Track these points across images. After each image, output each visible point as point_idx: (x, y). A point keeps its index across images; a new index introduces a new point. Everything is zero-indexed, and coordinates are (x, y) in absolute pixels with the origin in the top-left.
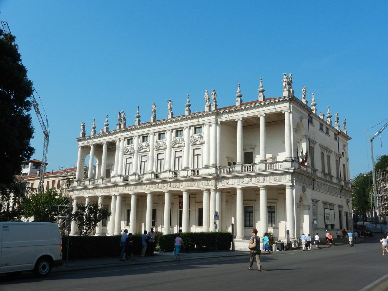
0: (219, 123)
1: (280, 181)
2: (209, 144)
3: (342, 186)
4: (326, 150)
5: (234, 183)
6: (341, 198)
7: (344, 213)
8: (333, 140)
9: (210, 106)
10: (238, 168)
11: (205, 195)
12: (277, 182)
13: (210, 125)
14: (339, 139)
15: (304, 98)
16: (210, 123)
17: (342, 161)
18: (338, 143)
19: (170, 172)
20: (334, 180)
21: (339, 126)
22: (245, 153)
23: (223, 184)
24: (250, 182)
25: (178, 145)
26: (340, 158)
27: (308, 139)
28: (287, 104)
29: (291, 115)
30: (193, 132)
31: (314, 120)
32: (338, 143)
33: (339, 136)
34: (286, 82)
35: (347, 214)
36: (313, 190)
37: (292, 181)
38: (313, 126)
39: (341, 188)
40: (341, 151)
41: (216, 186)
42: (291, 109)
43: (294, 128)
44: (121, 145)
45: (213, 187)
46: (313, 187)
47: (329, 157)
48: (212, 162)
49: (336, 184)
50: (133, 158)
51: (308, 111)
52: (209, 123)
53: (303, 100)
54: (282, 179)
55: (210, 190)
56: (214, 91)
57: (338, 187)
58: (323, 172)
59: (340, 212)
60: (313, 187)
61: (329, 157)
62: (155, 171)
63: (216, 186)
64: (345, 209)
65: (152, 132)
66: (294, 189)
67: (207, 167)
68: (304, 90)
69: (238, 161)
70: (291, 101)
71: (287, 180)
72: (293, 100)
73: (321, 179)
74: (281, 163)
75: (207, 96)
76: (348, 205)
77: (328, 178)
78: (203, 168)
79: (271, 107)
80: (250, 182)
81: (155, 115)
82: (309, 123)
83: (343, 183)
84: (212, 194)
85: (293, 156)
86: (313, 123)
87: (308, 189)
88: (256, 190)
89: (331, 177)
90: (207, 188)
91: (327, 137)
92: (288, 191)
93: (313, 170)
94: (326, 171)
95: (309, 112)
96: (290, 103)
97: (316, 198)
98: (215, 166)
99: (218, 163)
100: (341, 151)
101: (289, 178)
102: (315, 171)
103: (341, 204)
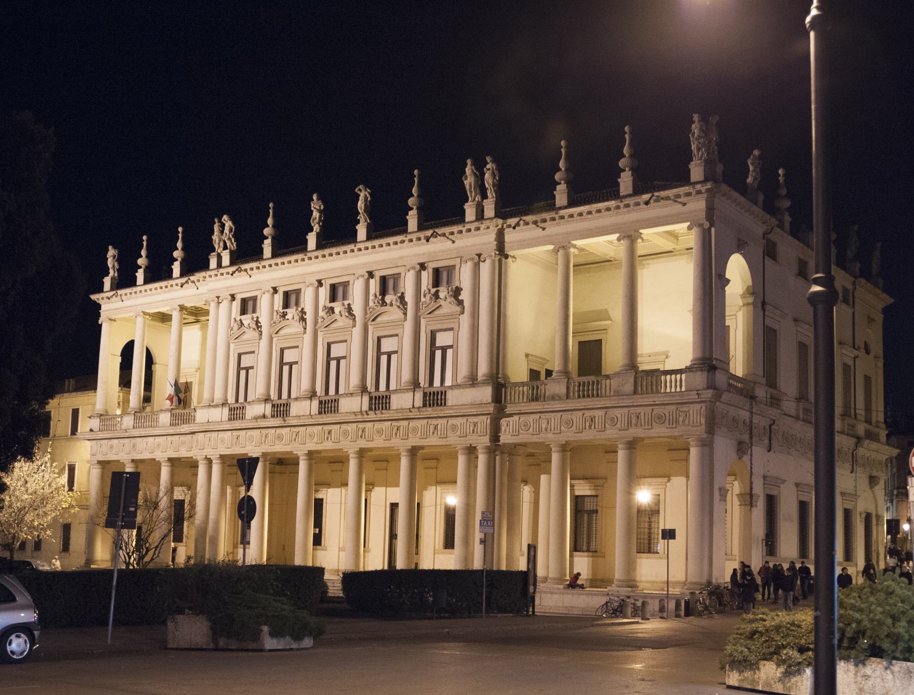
5: (546, 429)
16: (479, 255)
22: (580, 343)
30: (431, 282)
36: (769, 451)
50: (256, 352)
52: (477, 255)
62: (231, 399)
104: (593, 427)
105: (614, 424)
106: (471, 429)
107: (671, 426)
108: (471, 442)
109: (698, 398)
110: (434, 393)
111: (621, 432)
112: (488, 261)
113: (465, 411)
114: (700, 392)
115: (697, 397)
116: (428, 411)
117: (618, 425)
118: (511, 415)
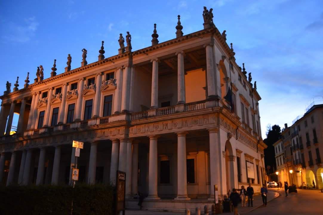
1: (202, 124)
2: (121, 88)
5: (147, 130)
10: (151, 113)
11: (114, 145)
14: (253, 97)
16: (123, 66)
19: (78, 123)
20: (252, 134)
24: (165, 128)
26: (255, 114)
36: (237, 139)
38: (234, 73)
40: (255, 109)
41: (127, 134)
45: (123, 136)
48: (123, 108)
54: (205, 122)
55: (119, 140)
57: (255, 141)
61: (247, 110)
63: (127, 134)
67: (118, 114)
69: (152, 104)
70: (213, 34)
74: (203, 104)
77: (248, 130)
78: (113, 115)
80: (165, 128)
84: (122, 144)
87: (232, 137)
88: (174, 137)
90: (116, 137)
94: (246, 122)
95: (230, 56)
97: (240, 149)
98: (126, 112)
103: (257, 158)
104: (167, 128)
105: (175, 126)
106: (117, 132)
107: (201, 125)
108: (117, 137)
109: (213, 111)
110: (104, 119)
111: (179, 129)
112: (126, 68)
113: (115, 124)
114: (213, 108)
115: (211, 111)
116: (100, 126)
117: (178, 127)
118: (133, 126)
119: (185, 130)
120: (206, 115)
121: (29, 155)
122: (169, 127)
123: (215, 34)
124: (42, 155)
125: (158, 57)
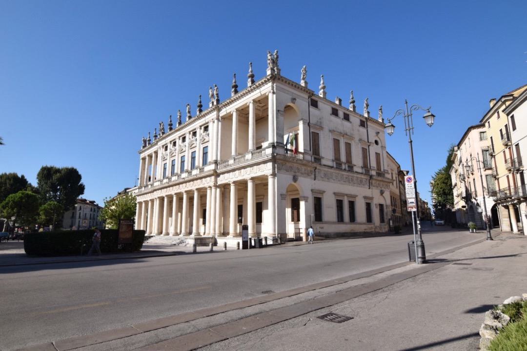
0: (220, 118)
2: (212, 140)
3: (371, 177)
4: (343, 136)
6: (369, 188)
7: (374, 206)
8: (358, 127)
9: (213, 103)
11: (208, 191)
12: (261, 173)
13: (214, 122)
14: (368, 126)
15: (303, 79)
17: (373, 149)
18: (367, 131)
21: (368, 113)
23: (222, 180)
25: (193, 146)
26: (369, 146)
27: (307, 124)
28: (270, 84)
29: (275, 96)
31: (320, 104)
32: (367, 131)
33: (368, 123)
34: (269, 60)
35: (381, 206)
37: (274, 168)
39: (369, 178)
41: (216, 181)
42: (275, 88)
43: (278, 111)
44: (161, 152)
46: (315, 177)
47: (348, 146)
49: (362, 173)
51: (307, 92)
53: (302, 83)
56: (216, 86)
58: (337, 159)
59: (368, 205)
60: (315, 177)
63: (216, 181)
64: (377, 200)
65: (177, 137)
66: (276, 178)
68: (303, 71)
70: (274, 79)
71: (267, 169)
72: (274, 78)
73: (332, 167)
75: (211, 93)
76: (383, 196)
79: (258, 91)
81: (180, 121)
82: (310, 106)
83: (373, 173)
85: (275, 141)
86: (318, 107)
89: (351, 168)
91: (346, 123)
92: (270, 181)
93: (315, 158)
94: (343, 158)
95: (310, 93)
96: (273, 83)
98: (216, 162)
99: (219, 159)
100: (372, 139)
101: (270, 165)
102: (318, 159)
119: (252, 176)
120: (265, 162)
121: (158, 201)
122: (242, 175)
123: (276, 80)
124: (143, 205)
125: (237, 107)
